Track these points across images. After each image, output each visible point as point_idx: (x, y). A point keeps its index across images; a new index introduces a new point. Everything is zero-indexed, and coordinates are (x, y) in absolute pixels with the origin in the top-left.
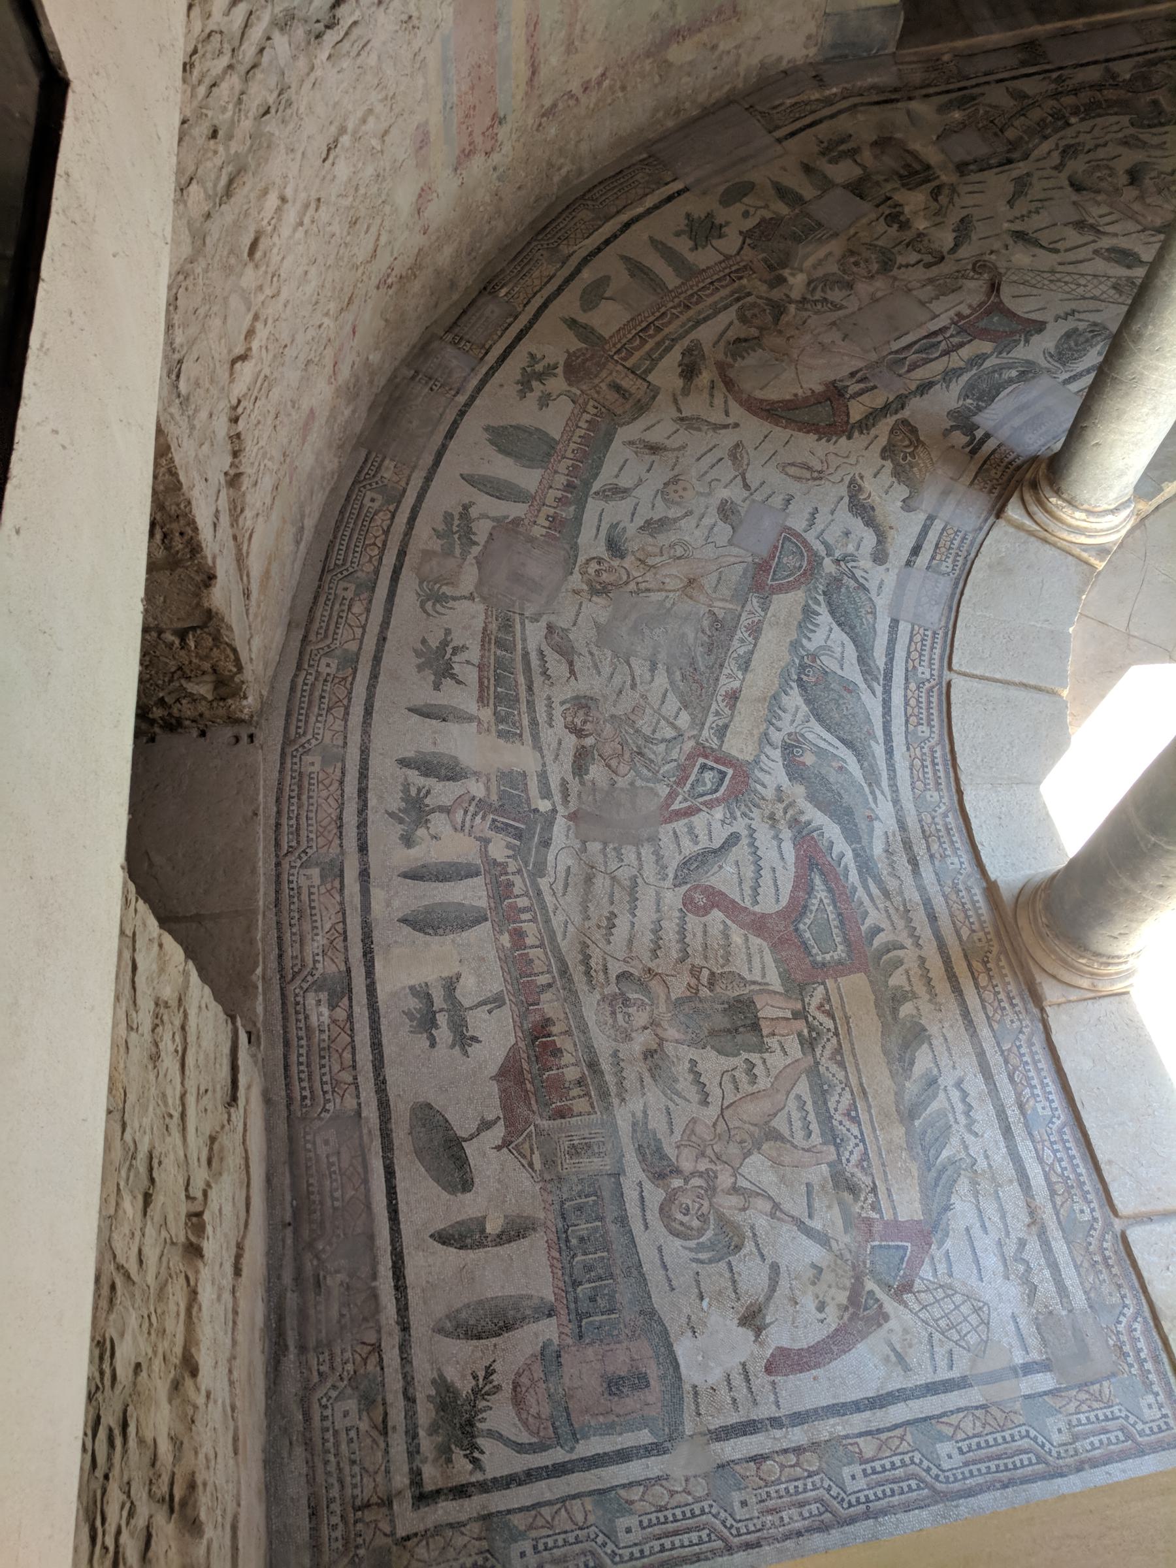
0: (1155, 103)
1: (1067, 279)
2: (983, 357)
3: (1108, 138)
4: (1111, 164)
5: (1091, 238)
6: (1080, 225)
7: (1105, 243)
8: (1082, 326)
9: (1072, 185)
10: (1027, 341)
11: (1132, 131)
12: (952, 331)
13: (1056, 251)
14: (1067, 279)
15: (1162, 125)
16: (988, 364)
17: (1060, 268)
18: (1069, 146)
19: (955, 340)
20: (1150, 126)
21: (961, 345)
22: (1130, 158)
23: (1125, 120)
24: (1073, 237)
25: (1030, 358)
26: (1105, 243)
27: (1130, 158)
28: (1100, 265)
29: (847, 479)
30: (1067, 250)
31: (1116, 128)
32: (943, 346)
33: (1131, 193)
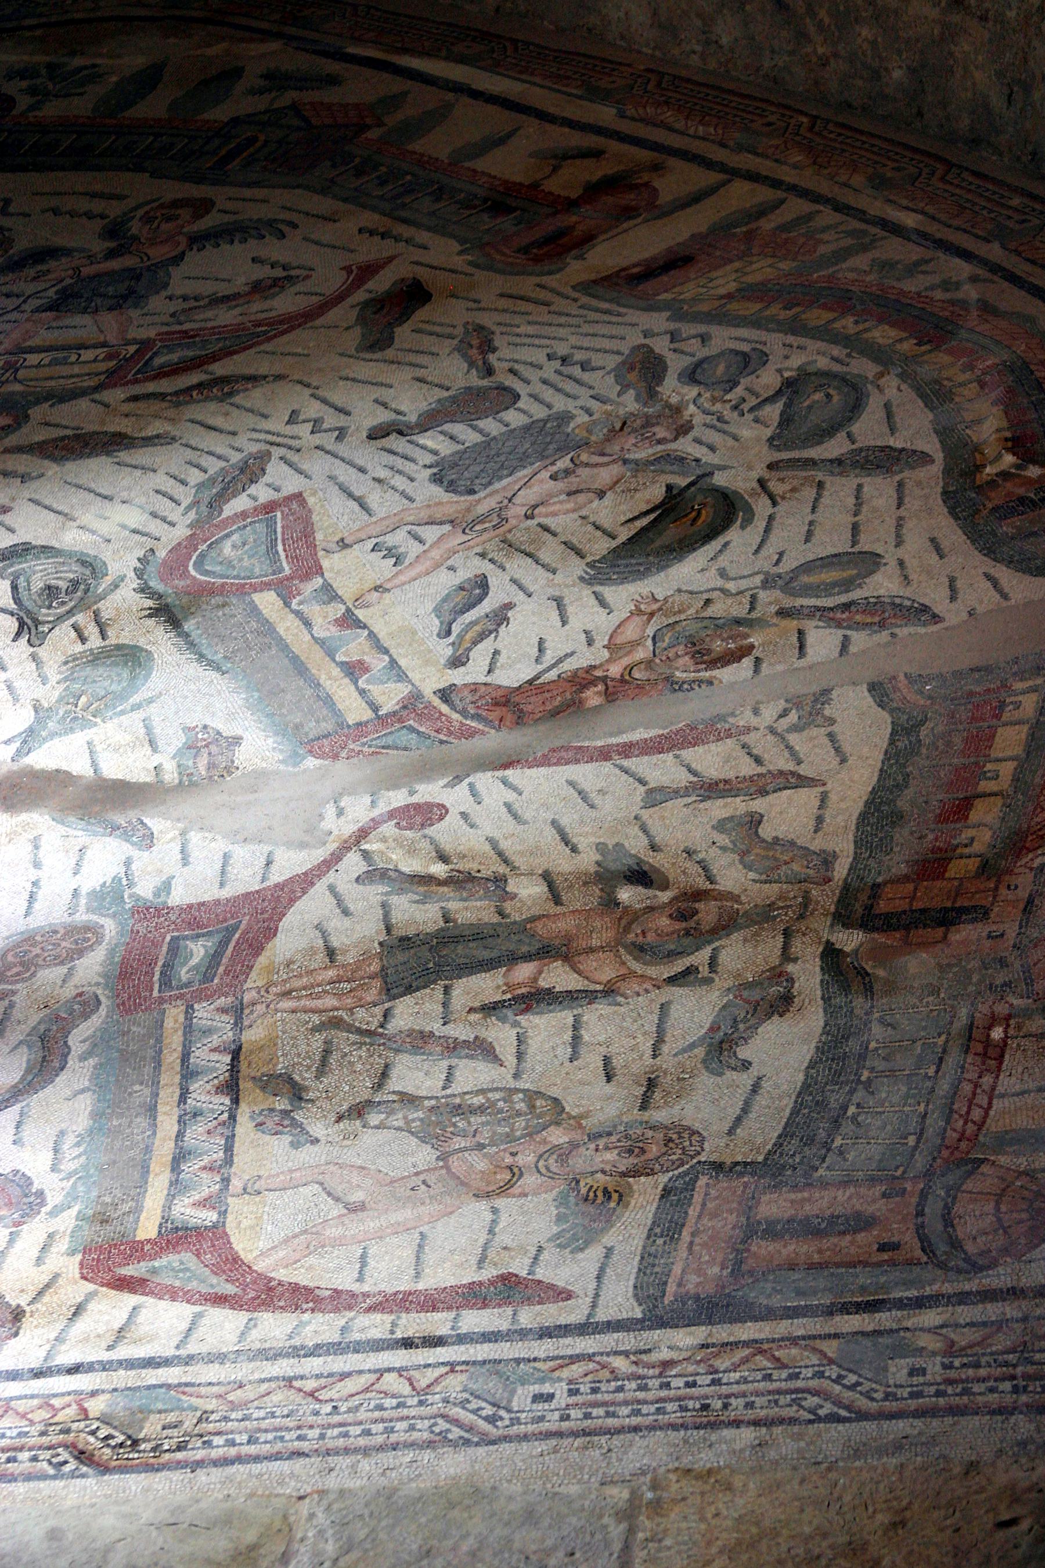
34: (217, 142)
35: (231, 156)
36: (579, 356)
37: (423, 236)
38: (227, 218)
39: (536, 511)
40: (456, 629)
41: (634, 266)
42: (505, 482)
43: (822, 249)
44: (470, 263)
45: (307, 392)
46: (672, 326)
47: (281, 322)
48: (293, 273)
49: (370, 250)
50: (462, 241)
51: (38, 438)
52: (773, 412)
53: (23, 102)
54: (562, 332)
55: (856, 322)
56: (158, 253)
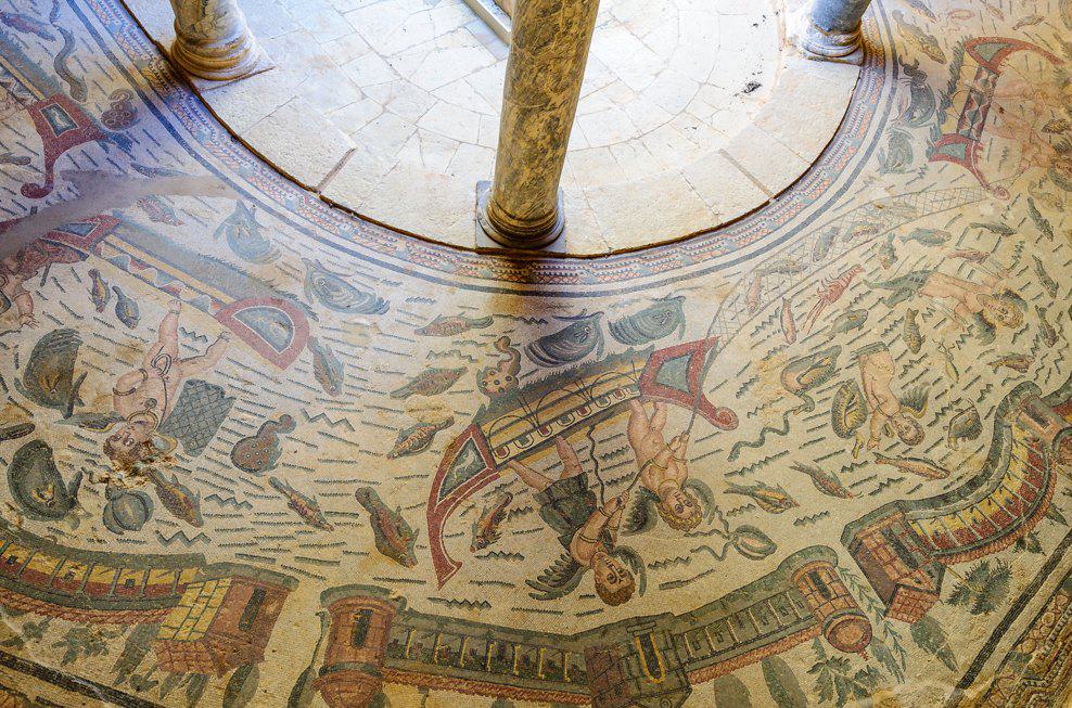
0: (1043, 422)
1: (947, 203)
2: (943, 119)
3: (1038, 360)
4: (1011, 332)
5: (962, 247)
6: (980, 258)
7: (950, 247)
8: (908, 168)
9: (1017, 296)
10: (928, 142)
11: (1030, 376)
12: (974, 133)
13: (975, 226)
14: (947, 203)
15: (1015, 393)
16: (935, 116)
17: (958, 210)
18: (1055, 340)
19: (966, 128)
20: (1020, 388)
21: (960, 126)
22: (1003, 344)
23: (1046, 391)
24: (971, 243)
25: (918, 130)
26: (950, 247)
27: (1003, 344)
28: (938, 223)
29: (938, 19)
30: (967, 229)
31: (1043, 374)
32: (968, 121)
33: (974, 304)
34: (675, 664)
35: (651, 657)
36: (230, 508)
37: (442, 610)
38: (579, 591)
39: (141, 376)
40: (112, 293)
41: (276, 614)
42: (178, 394)
43: (151, 658)
44: (387, 592)
45: (363, 447)
46: (193, 550)
47: (446, 505)
48: (484, 552)
49: (457, 587)
50: (412, 613)
51: (462, 380)
52: (68, 477)
53: (831, 652)
54: (263, 531)
55: (70, 574)
56: (581, 550)
